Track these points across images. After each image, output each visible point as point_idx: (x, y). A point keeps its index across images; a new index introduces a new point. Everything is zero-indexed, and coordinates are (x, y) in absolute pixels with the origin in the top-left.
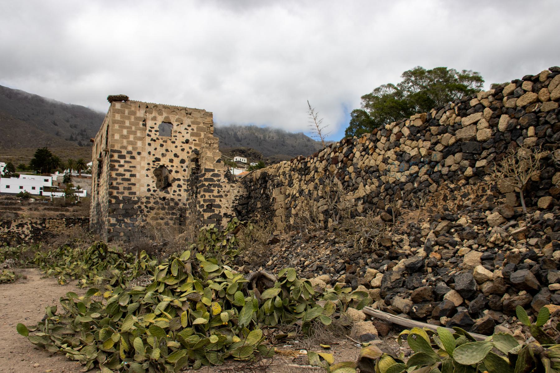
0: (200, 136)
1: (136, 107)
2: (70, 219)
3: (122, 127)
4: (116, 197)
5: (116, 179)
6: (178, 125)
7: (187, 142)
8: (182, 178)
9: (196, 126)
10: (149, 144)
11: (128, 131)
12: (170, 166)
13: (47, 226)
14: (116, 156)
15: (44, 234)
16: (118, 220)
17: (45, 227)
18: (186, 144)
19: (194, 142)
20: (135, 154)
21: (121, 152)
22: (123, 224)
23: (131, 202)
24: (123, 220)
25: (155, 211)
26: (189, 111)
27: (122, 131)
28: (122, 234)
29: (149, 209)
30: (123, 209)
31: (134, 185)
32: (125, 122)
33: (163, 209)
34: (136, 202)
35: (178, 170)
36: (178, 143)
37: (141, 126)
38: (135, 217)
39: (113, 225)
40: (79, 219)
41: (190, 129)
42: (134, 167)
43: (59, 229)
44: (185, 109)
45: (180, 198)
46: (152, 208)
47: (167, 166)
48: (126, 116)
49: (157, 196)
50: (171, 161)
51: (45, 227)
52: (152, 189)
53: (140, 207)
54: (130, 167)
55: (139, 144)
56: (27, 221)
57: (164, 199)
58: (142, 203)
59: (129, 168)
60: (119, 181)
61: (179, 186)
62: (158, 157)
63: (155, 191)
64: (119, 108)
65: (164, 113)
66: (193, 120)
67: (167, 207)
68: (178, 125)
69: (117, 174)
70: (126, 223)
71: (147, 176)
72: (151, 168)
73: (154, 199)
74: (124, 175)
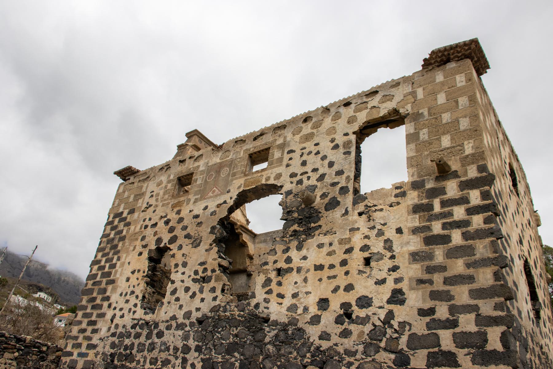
40: (19, 340)
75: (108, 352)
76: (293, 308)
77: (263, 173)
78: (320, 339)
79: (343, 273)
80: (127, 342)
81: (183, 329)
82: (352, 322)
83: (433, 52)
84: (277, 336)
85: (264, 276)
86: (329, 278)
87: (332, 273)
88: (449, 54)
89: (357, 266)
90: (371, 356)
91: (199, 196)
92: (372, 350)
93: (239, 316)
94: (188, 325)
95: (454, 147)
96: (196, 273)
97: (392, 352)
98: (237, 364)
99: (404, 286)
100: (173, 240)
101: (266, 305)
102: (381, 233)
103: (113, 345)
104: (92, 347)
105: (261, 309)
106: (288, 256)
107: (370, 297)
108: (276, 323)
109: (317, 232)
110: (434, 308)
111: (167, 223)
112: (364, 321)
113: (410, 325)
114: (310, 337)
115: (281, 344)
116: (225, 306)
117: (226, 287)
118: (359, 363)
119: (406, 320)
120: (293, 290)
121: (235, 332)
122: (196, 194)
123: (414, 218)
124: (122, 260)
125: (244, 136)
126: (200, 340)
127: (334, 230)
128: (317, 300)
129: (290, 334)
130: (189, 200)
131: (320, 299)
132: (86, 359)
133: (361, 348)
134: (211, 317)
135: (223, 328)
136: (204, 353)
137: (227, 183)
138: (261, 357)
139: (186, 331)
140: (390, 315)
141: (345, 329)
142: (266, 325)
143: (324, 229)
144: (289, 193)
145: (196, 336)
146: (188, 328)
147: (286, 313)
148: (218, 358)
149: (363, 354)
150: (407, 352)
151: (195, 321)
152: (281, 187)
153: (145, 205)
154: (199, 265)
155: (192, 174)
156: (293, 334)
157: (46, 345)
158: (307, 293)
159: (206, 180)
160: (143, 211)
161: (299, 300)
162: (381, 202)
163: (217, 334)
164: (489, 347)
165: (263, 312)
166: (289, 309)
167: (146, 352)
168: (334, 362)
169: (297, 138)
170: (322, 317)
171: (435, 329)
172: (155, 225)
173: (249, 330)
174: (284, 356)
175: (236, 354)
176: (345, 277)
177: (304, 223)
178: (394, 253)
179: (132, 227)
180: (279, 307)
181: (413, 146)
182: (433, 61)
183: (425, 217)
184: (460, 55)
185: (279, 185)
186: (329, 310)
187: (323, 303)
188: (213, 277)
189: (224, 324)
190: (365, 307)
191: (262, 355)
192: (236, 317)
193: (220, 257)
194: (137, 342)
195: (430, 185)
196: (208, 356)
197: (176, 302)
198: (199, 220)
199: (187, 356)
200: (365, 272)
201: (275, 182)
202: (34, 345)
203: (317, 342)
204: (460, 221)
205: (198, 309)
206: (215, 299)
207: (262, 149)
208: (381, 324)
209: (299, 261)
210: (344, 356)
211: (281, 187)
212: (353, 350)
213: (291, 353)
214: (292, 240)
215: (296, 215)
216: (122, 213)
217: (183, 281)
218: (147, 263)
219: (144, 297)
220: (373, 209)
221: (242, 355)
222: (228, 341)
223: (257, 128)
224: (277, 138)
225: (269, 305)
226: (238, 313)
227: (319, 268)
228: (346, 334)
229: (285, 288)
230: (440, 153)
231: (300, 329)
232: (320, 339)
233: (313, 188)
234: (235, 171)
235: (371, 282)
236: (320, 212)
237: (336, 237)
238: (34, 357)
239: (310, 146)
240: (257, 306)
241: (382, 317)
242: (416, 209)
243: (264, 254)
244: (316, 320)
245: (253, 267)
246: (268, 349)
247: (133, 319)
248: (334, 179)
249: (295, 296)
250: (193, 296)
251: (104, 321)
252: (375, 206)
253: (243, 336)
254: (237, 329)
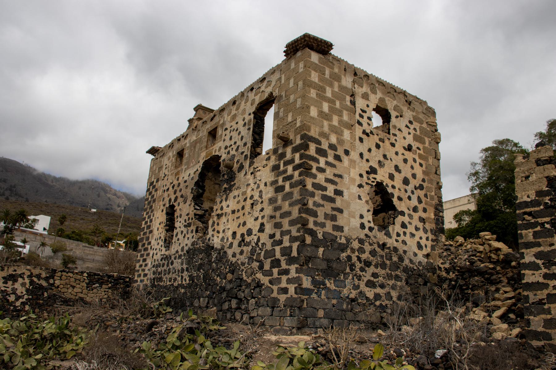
0: (423, 143)
1: (340, 68)
2: (95, 274)
3: (322, 97)
4: (312, 233)
5: (313, 195)
6: (397, 117)
7: (409, 148)
8: (406, 211)
9: (419, 125)
10: (361, 140)
11: (329, 107)
12: (390, 185)
13: (57, 282)
14: (312, 150)
15: (49, 297)
16: (314, 282)
17: (53, 285)
18: (408, 152)
19: (418, 151)
20: (340, 152)
21: (319, 143)
22: (323, 292)
23: (336, 246)
24: (324, 284)
25: (372, 269)
26: (411, 99)
27: (321, 103)
28: (321, 313)
29: (362, 265)
30: (323, 259)
31: (341, 211)
32: (325, 89)
33: (383, 266)
34: (343, 248)
35: (402, 196)
36: (399, 147)
37: (348, 103)
38: (342, 277)
39: (307, 292)
40: (109, 277)
41: (412, 127)
42: (340, 176)
43: (75, 290)
44: (404, 93)
45: (405, 248)
46: (368, 264)
47: (387, 185)
48: (327, 79)
49: (375, 241)
50: (391, 177)
51: (53, 285)
52: (367, 225)
53: (349, 258)
54: (335, 175)
55: (347, 134)
56: (24, 271)
57: (383, 246)
58: (353, 251)
59: (331, 177)
60: (317, 199)
61: (404, 226)
62: (373, 166)
63: (371, 229)
64: (317, 62)
65: (378, 92)
66: (414, 114)
67: (388, 262)
68: (397, 117)
69: (314, 185)
70: (329, 289)
71: (360, 198)
72: (364, 184)
73: (371, 245)
74: (325, 189)
80: (159, 270)
83: (287, 47)
84: (217, 257)
98: (202, 276)
100: (176, 200)
104: (145, 275)
111: (173, 187)
117: (199, 229)
124: (155, 216)
130: (182, 169)
137: (199, 156)
153: (163, 175)
155: (183, 149)
157: (128, 277)
164: (292, 255)
172: (168, 189)
175: (201, 270)
179: (158, 192)
181: (276, 122)
193: (195, 209)
194: (163, 269)
199: (183, 274)
202: (120, 278)
216: (153, 182)
218: (165, 216)
219: (165, 240)
238: (122, 286)
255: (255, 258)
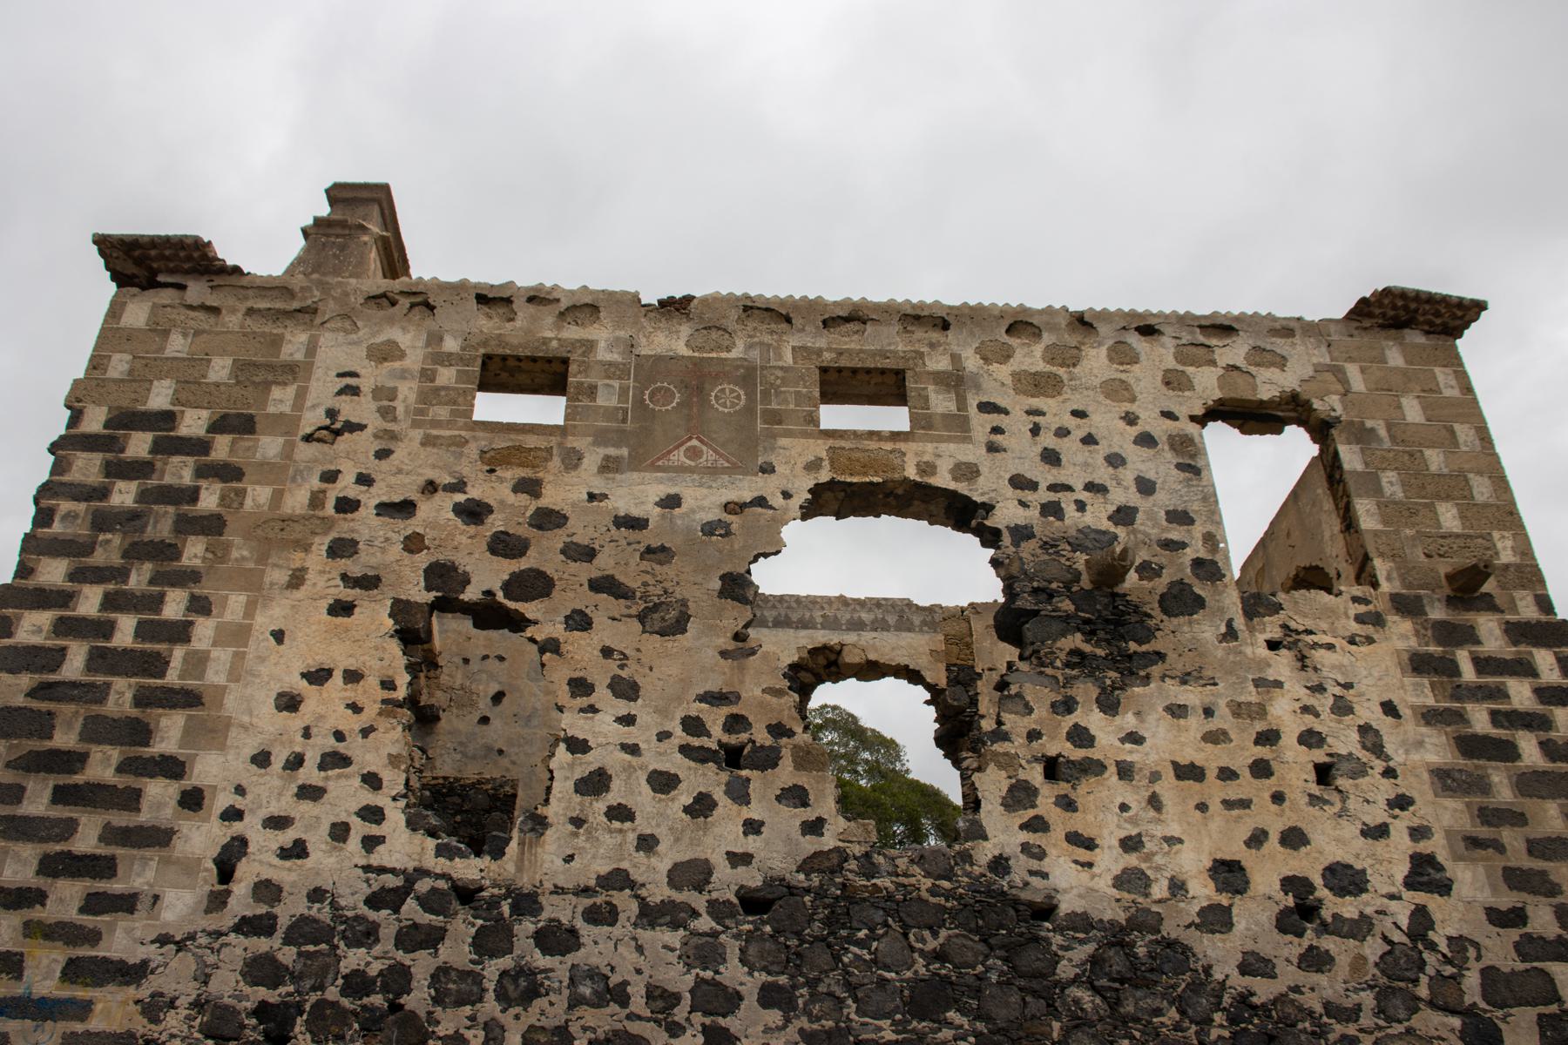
75: (240, 999)
76: (1131, 880)
77: (902, 446)
78: (1243, 973)
79: (1267, 796)
81: (675, 925)
82: (1324, 928)
83: (1387, 292)
84: (1095, 960)
85: (1004, 774)
86: (1228, 804)
87: (1233, 791)
88: (1416, 311)
89: (1301, 783)
90: (1400, 1022)
91: (625, 452)
92: (1397, 1006)
93: (933, 891)
94: (702, 910)
95: (1470, 536)
96: (693, 725)
97: (1454, 1012)
99: (1436, 846)
101: (1034, 864)
102: (1342, 708)
103: (261, 970)
105: (1018, 873)
106: (1076, 726)
107: (1358, 867)
108: (1082, 923)
109: (1156, 670)
110: (1522, 909)
112: (1359, 928)
113: (1476, 945)
114: (1210, 967)
115: (1117, 985)
116: (867, 855)
118: (1373, 1038)
119: (1465, 932)
120: (1118, 826)
121: (932, 944)
122: (601, 438)
123: (1417, 684)
125: (782, 302)
126: (775, 968)
127: (1208, 673)
128: (1209, 864)
129: (1139, 956)
131: (1215, 861)
132: (79, 1027)
133: (1368, 999)
134: (808, 891)
135: (872, 930)
136: (809, 1015)
138: (1056, 1025)
139: (694, 933)
140: (1421, 918)
141: (1311, 948)
142: (1047, 924)
143: (1176, 663)
144: (1022, 533)
145: (753, 950)
146: (705, 923)
147: (1115, 893)
148: (880, 1029)
149: (1377, 1015)
150: (1486, 1011)
151: (735, 901)
152: (988, 508)
154: (702, 698)
156: (1151, 955)
158: (1171, 841)
159: (639, 402)
160: (308, 438)
161: (1148, 857)
162: (1324, 626)
163: (854, 949)
165: (1026, 884)
166: (1121, 881)
167: (490, 1006)
168: (1303, 1037)
169: (1003, 372)
170: (1235, 911)
171: (1538, 959)
173: (984, 941)
174: (1137, 1020)
176: (1274, 808)
177: (1101, 634)
178: (1391, 764)
180: (1084, 875)
182: (1377, 311)
183: (1445, 690)
184: (1438, 321)
185: (978, 499)
186: (1250, 893)
187: (1228, 873)
188: (786, 753)
189: (878, 916)
190: (1350, 893)
191: (1058, 1019)
192: (925, 895)
195: (1437, 613)
196: (829, 1024)
197: (616, 824)
198: (649, 538)
200: (1327, 802)
201: (962, 488)
203: (1238, 982)
204: (1528, 714)
205: (739, 859)
206: (814, 827)
207: (870, 364)
208: (1405, 939)
209: (1118, 743)
210: (1325, 1019)
211: (988, 508)
212: (1348, 1003)
213: (1158, 1012)
214: (1075, 678)
215: (1067, 606)
217: (633, 749)
220: (1309, 639)
221: (978, 1018)
222: (909, 974)
223: (836, 289)
224: (925, 349)
225: (1045, 865)
226: (928, 882)
227: (1189, 772)
228: (1315, 960)
229: (1090, 818)
230: (1441, 541)
231: (1171, 944)
232: (1243, 973)
233: (1106, 538)
234: (774, 406)
235: (1351, 830)
236: (1150, 616)
237: (1219, 695)
239: (1056, 411)
240: (1000, 864)
241: (1404, 922)
242: (1419, 664)
243: (485, 657)
244: (1216, 919)
245: (439, 694)
246: (1077, 1001)
247: (367, 868)
248: (1164, 530)
249: (1130, 844)
250: (702, 807)
251: (166, 862)
252: (1310, 632)
253: (970, 957)
254: (935, 935)
255: (1423, 991)
